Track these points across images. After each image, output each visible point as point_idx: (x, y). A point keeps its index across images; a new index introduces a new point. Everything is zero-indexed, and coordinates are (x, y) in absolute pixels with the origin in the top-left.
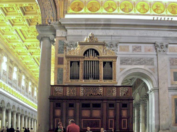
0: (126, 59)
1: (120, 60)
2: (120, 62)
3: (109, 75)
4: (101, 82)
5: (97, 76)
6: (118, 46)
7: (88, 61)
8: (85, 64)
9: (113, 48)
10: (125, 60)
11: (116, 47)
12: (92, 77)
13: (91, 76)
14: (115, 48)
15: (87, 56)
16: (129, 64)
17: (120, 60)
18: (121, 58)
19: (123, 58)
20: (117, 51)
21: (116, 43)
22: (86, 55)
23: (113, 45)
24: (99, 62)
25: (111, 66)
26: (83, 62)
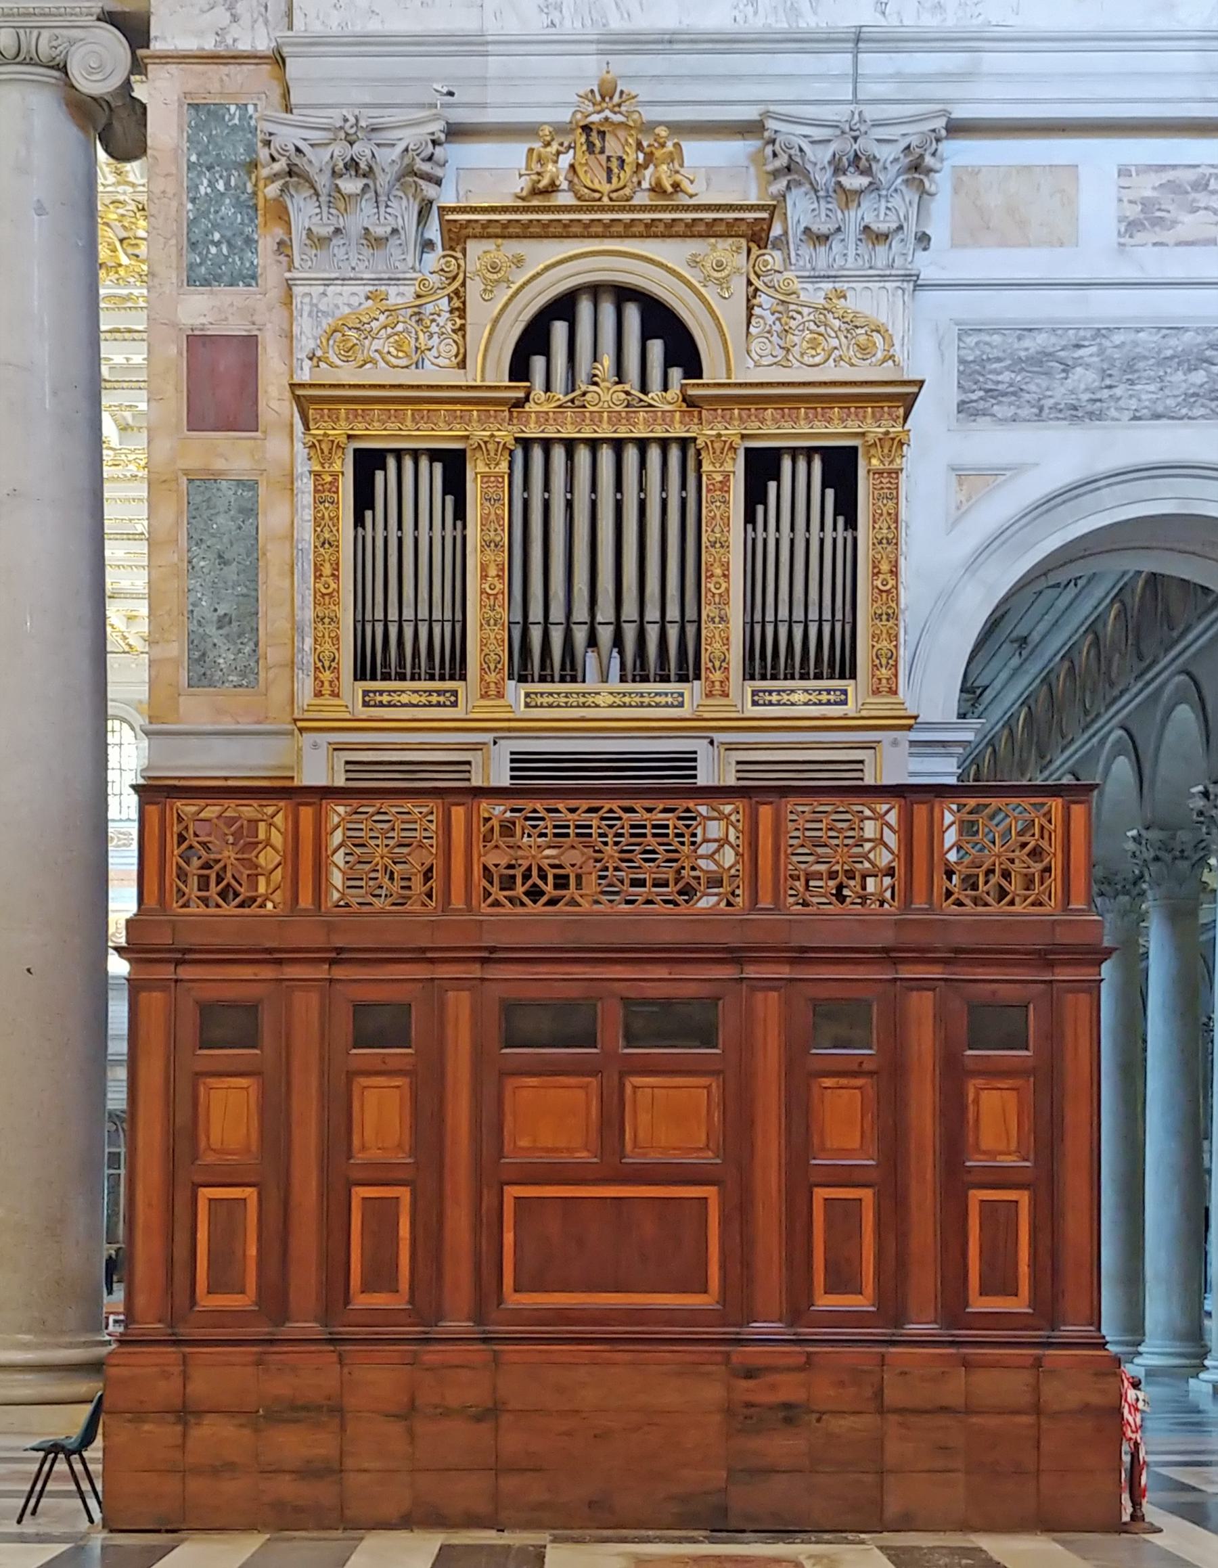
0: (1033, 344)
1: (954, 367)
2: (954, 396)
3: (813, 614)
4: (715, 709)
5: (673, 633)
6: (941, 183)
7: (570, 445)
8: (526, 486)
9: (869, 213)
10: (1019, 364)
11: (912, 195)
12: (618, 641)
13: (605, 635)
14: (896, 201)
15: (548, 388)
16: (1075, 413)
17: (962, 361)
18: (971, 340)
19: (996, 339)
20: (923, 240)
21: (913, 134)
22: (538, 362)
23: (867, 172)
24: (698, 453)
25: (847, 508)
26: (504, 466)
